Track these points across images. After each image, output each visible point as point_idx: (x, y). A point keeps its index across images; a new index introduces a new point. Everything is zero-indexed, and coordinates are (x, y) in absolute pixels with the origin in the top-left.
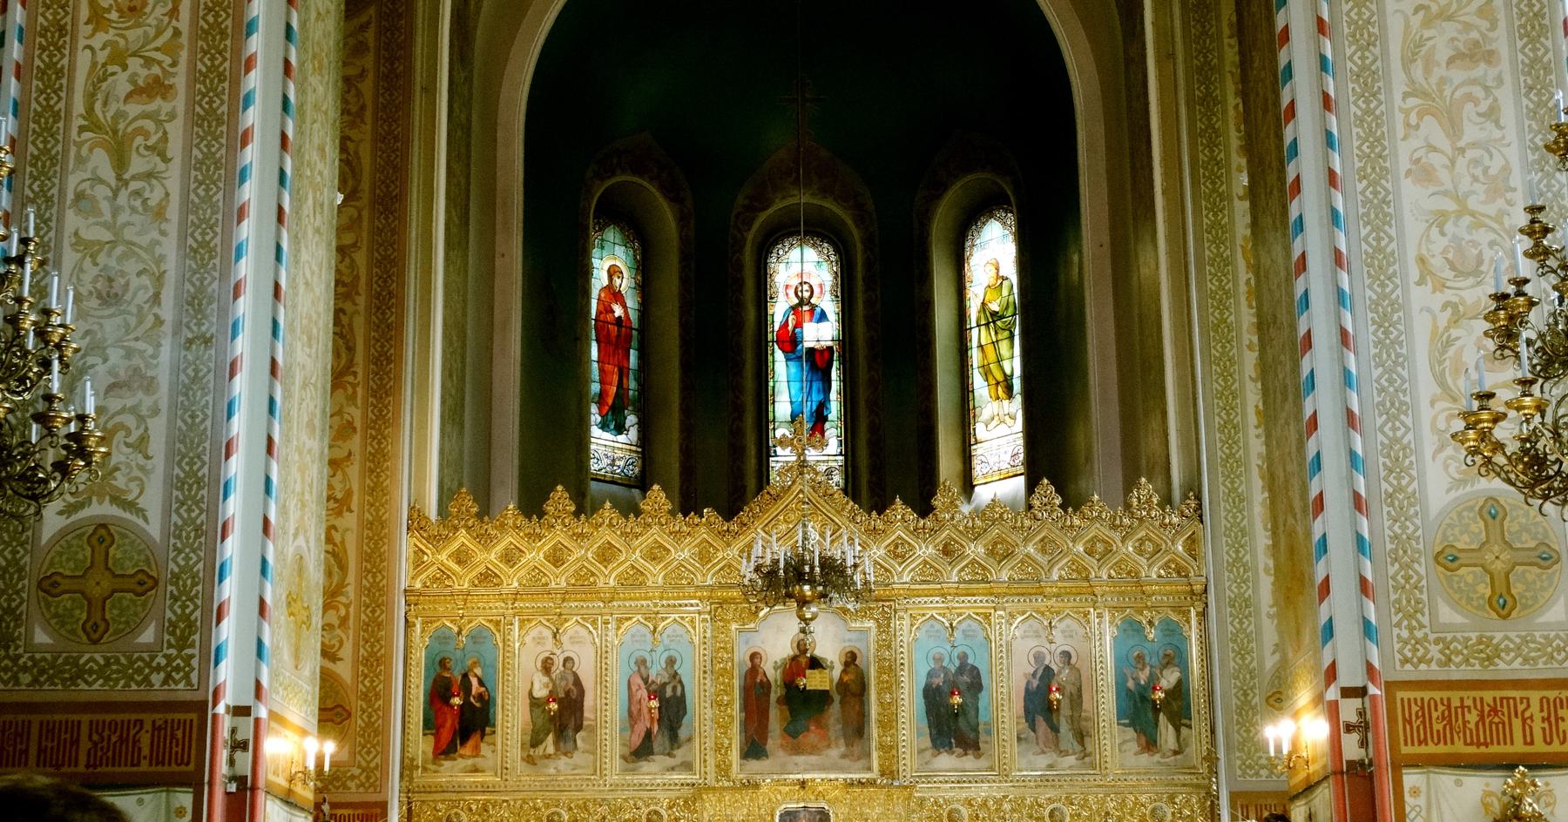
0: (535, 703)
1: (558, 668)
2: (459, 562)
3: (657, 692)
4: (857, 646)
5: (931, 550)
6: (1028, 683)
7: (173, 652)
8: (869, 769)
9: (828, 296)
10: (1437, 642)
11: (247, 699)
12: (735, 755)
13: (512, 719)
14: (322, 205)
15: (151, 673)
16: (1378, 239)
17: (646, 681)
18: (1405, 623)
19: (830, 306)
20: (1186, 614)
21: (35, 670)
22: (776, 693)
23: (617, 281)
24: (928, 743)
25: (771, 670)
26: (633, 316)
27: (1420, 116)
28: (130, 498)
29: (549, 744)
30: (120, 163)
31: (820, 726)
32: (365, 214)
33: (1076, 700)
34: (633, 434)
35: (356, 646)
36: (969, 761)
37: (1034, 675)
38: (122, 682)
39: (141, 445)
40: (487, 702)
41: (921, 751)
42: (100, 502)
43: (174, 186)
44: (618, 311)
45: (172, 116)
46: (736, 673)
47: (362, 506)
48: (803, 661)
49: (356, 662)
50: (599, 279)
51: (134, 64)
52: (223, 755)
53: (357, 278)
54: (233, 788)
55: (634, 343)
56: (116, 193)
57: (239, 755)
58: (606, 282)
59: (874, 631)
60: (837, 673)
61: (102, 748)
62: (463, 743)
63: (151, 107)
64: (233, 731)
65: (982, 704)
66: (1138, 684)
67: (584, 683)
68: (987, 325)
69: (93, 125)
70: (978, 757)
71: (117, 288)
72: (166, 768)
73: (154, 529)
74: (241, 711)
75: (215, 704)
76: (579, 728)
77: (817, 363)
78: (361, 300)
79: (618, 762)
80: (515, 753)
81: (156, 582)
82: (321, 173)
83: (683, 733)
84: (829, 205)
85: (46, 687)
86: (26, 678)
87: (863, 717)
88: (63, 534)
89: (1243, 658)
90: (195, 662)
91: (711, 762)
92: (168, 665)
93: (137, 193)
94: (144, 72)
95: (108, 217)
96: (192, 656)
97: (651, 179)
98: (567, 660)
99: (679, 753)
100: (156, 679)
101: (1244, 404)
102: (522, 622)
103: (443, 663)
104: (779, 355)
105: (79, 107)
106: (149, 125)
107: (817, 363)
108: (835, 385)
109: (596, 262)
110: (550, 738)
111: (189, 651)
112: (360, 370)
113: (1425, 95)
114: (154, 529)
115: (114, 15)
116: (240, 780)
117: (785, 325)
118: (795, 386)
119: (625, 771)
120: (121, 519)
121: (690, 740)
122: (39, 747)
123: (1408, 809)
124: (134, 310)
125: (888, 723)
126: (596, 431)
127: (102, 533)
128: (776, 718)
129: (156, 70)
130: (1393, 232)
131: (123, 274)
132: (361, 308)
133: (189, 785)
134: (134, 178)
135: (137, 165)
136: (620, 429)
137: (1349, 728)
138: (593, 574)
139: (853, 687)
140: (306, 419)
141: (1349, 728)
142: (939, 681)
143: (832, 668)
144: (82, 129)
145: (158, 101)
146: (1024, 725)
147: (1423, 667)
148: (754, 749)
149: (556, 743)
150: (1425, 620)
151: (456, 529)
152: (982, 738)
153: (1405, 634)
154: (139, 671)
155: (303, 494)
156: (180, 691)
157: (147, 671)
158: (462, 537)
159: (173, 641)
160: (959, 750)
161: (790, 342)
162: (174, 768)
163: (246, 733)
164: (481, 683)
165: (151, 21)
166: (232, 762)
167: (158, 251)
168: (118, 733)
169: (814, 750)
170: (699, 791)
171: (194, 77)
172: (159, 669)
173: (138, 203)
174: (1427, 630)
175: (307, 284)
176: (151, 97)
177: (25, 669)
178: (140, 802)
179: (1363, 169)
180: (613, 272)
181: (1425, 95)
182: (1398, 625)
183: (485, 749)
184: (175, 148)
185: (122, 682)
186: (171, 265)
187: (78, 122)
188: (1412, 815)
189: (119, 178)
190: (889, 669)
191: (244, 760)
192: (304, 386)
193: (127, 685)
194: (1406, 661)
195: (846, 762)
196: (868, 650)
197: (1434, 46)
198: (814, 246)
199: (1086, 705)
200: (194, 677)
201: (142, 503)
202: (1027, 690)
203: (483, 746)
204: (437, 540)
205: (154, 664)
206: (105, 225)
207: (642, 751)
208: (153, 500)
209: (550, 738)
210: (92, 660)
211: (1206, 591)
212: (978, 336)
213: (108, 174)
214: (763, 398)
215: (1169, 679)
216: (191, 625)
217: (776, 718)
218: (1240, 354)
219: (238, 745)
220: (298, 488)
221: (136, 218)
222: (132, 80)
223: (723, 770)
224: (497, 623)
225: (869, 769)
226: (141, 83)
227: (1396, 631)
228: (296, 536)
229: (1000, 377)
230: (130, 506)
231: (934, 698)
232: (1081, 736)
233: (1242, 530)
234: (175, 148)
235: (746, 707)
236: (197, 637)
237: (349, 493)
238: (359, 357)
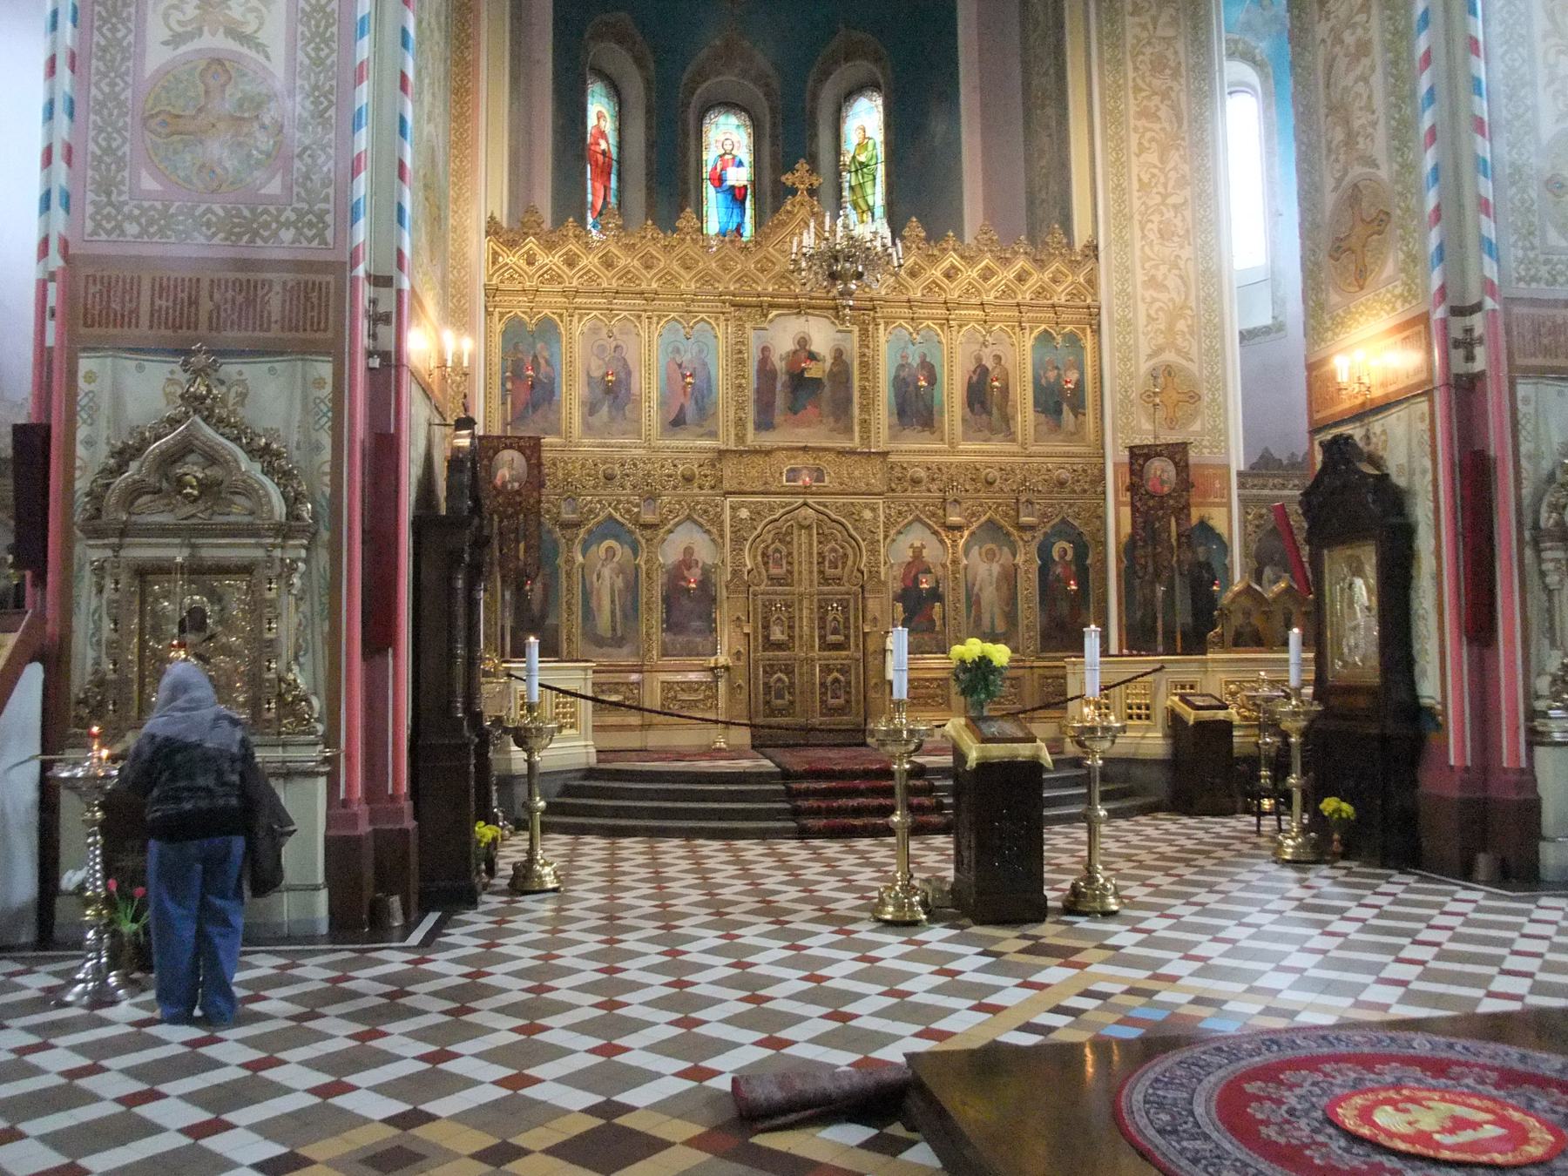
6: (971, 378)
8: (852, 439)
10: (1546, 262)
11: (390, 269)
12: (750, 427)
15: (279, 229)
18: (1520, 244)
20: (1084, 330)
21: (143, 220)
22: (782, 378)
24: (895, 419)
33: (1005, 390)
37: (974, 372)
38: (246, 238)
41: (890, 427)
42: (213, 34)
48: (803, 355)
50: (592, 121)
52: (363, 325)
54: (376, 363)
57: (382, 329)
61: (225, 310)
64: (374, 302)
68: (856, 171)
72: (301, 335)
74: (380, 281)
85: (156, 239)
86: (132, 229)
89: (1125, 365)
90: (329, 218)
91: (732, 431)
92: (298, 220)
98: (617, 347)
101: (1129, 172)
107: (736, 196)
110: (605, 409)
116: (384, 356)
122: (152, 303)
123: (1520, 416)
128: (780, 400)
133: (328, 354)
137: (1457, 344)
138: (638, 278)
141: (1457, 344)
142: (902, 374)
147: (1534, 285)
148: (764, 424)
150: (1537, 242)
152: (936, 417)
153: (1520, 253)
157: (274, 226)
159: (303, 194)
160: (920, 428)
162: (309, 335)
163: (387, 304)
164: (547, 361)
166: (373, 336)
168: (244, 294)
170: (722, 454)
174: (1538, 252)
177: (130, 217)
178: (272, 371)
182: (1515, 245)
185: (246, 238)
188: (1523, 422)
191: (387, 333)
193: (252, 241)
194: (1519, 279)
196: (852, 349)
198: (735, 114)
202: (969, 383)
205: (283, 219)
207: (677, 423)
209: (605, 409)
210: (209, 210)
211: (1099, 314)
215: (1073, 376)
217: (780, 400)
218: (1128, 136)
219: (378, 319)
223: (740, 438)
224: (561, 316)
229: (865, 208)
232: (1007, 420)
233: (1127, 268)
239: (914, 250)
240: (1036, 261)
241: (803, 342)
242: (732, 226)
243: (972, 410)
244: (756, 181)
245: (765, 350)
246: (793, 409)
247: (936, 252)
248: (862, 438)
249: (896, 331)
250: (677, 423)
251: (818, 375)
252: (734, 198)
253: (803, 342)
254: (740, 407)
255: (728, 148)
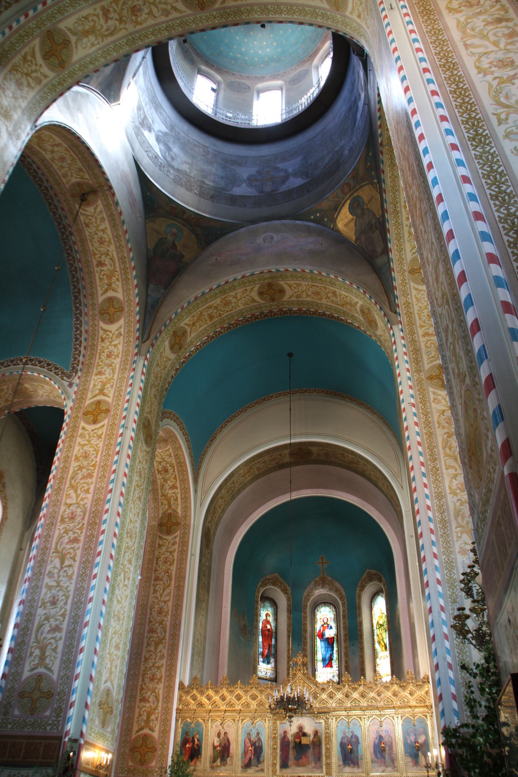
0: (214, 747)
1: (222, 735)
2: (194, 700)
3: (253, 744)
4: (319, 729)
5: (341, 696)
7: (54, 719)
8: (322, 772)
9: (333, 622)
11: (77, 736)
13: (207, 752)
14: (129, 579)
16: (450, 574)
17: (250, 740)
19: (333, 624)
20: (426, 716)
23: (268, 618)
24: (341, 763)
25: (290, 737)
26: (273, 628)
27: (461, 533)
28: (49, 666)
29: (218, 762)
30: (62, 562)
31: (306, 757)
32: (172, 591)
34: (273, 664)
35: (160, 728)
36: (355, 770)
39: (55, 650)
40: (199, 747)
41: (339, 766)
43: (76, 569)
44: (269, 627)
45: (78, 548)
46: (279, 738)
47: (165, 681)
48: (301, 734)
49: (159, 732)
50: (263, 617)
51: (70, 533)
53: (168, 610)
55: (274, 636)
56: (60, 571)
58: (265, 618)
59: (324, 723)
60: (311, 738)
62: (192, 760)
63: (73, 546)
65: (359, 748)
66: (411, 741)
67: (231, 741)
69: (56, 551)
70: (358, 768)
71: (55, 600)
73: (55, 677)
75: (65, 737)
76: (228, 756)
77: (329, 642)
78: (169, 617)
79: (240, 768)
80: (208, 765)
81: (53, 695)
82: (129, 569)
83: (261, 759)
84: (332, 594)
87: (320, 753)
88: (28, 678)
90: (61, 722)
91: (271, 769)
93: (65, 571)
94: (73, 536)
95: (56, 578)
96: (60, 721)
97: (278, 587)
99: (260, 766)
100: (49, 728)
102: (212, 720)
103: (187, 733)
104: (318, 640)
105: (53, 546)
106: (72, 551)
107: (329, 642)
108: (335, 649)
109: (262, 612)
110: (219, 760)
111: (59, 719)
112: (167, 638)
113: (462, 527)
114: (55, 677)
115: (67, 520)
117: (320, 631)
118: (323, 649)
119: (242, 772)
120: (46, 673)
121: (263, 761)
124: (59, 606)
125: (328, 757)
126: (261, 663)
127: (40, 677)
129: (76, 535)
130: (455, 572)
131: (58, 596)
132: (169, 619)
134: (65, 567)
135: (67, 563)
136: (268, 663)
139: (317, 743)
140: (114, 645)
142: (345, 741)
143: (310, 736)
144: (53, 552)
145: (75, 544)
146: (373, 756)
148: (284, 765)
149: (221, 761)
151: (193, 688)
152: (360, 761)
154: (43, 725)
155: (111, 669)
156: (55, 733)
158: (195, 692)
160: (352, 765)
161: (321, 636)
164: (198, 740)
165: (77, 521)
167: (69, 589)
169: (304, 765)
171: (86, 537)
172: (49, 724)
173: (65, 574)
175: (118, 601)
176: (74, 543)
179: (444, 552)
180: (267, 615)
181: (462, 527)
182: (466, 711)
183: (198, 763)
184: (78, 558)
186: (71, 593)
187: (52, 550)
189: (61, 567)
190: (328, 737)
192: (115, 633)
195: (315, 770)
197: (464, 512)
199: (394, 749)
200: (60, 728)
201: (53, 668)
203: (198, 763)
204: (187, 693)
206: (55, 581)
207: (247, 765)
208: (56, 668)
212: (377, 632)
213: (58, 566)
214: (314, 653)
216: (61, 710)
220: (108, 666)
221: (64, 579)
222: (69, 538)
224: (204, 720)
225: (322, 772)
226: (71, 539)
227: (465, 713)
228: (106, 682)
229: (383, 644)
230: (49, 669)
231: (343, 745)
232: (393, 760)
234: (78, 558)
235: (282, 750)
236: (62, 714)
237: (161, 677)
238: (167, 635)
239: (347, 686)
240: (401, 687)
241: (301, 728)
242: (328, 655)
243: (376, 757)
244: (338, 635)
245: (285, 732)
246: (297, 759)
247: (357, 686)
248: (326, 771)
249: (340, 722)
250: (247, 765)
251: (308, 743)
252: (328, 643)
253: (301, 728)
254: (275, 758)
255: (325, 621)
